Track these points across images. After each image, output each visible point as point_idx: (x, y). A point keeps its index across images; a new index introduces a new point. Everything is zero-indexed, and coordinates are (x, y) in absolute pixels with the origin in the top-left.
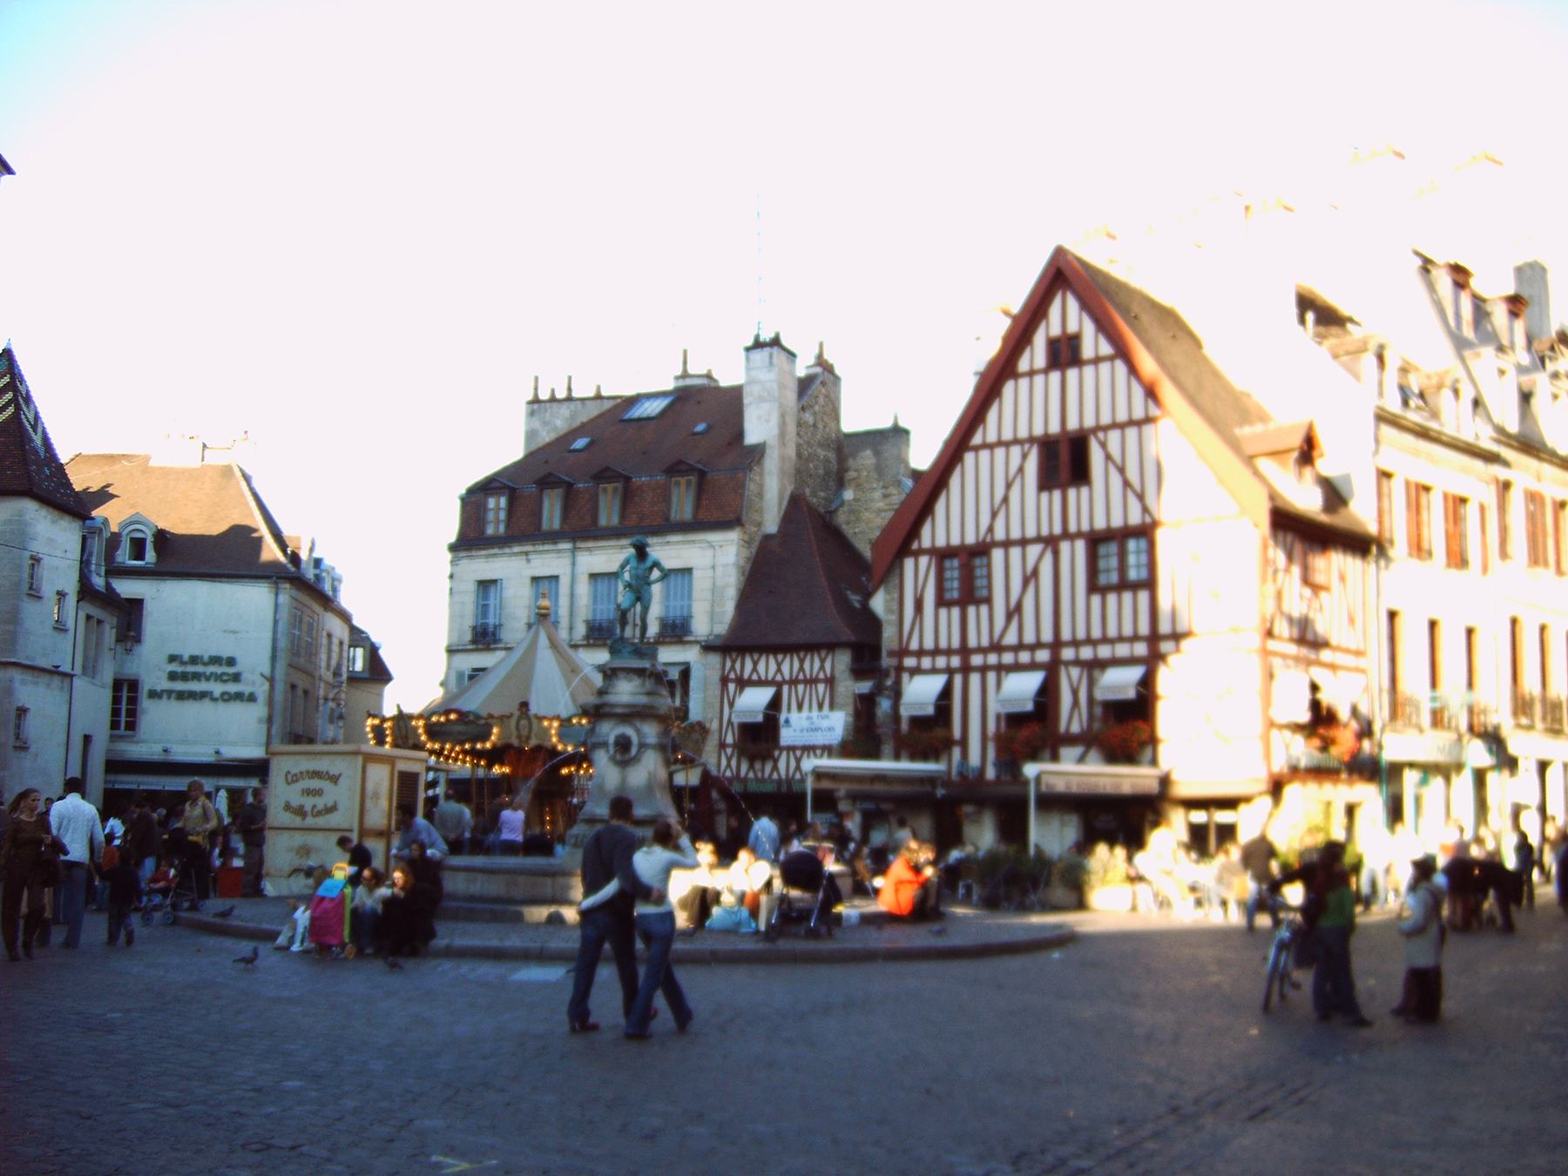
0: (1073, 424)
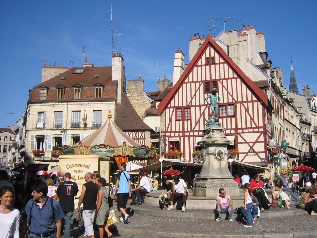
0: (213, 78)
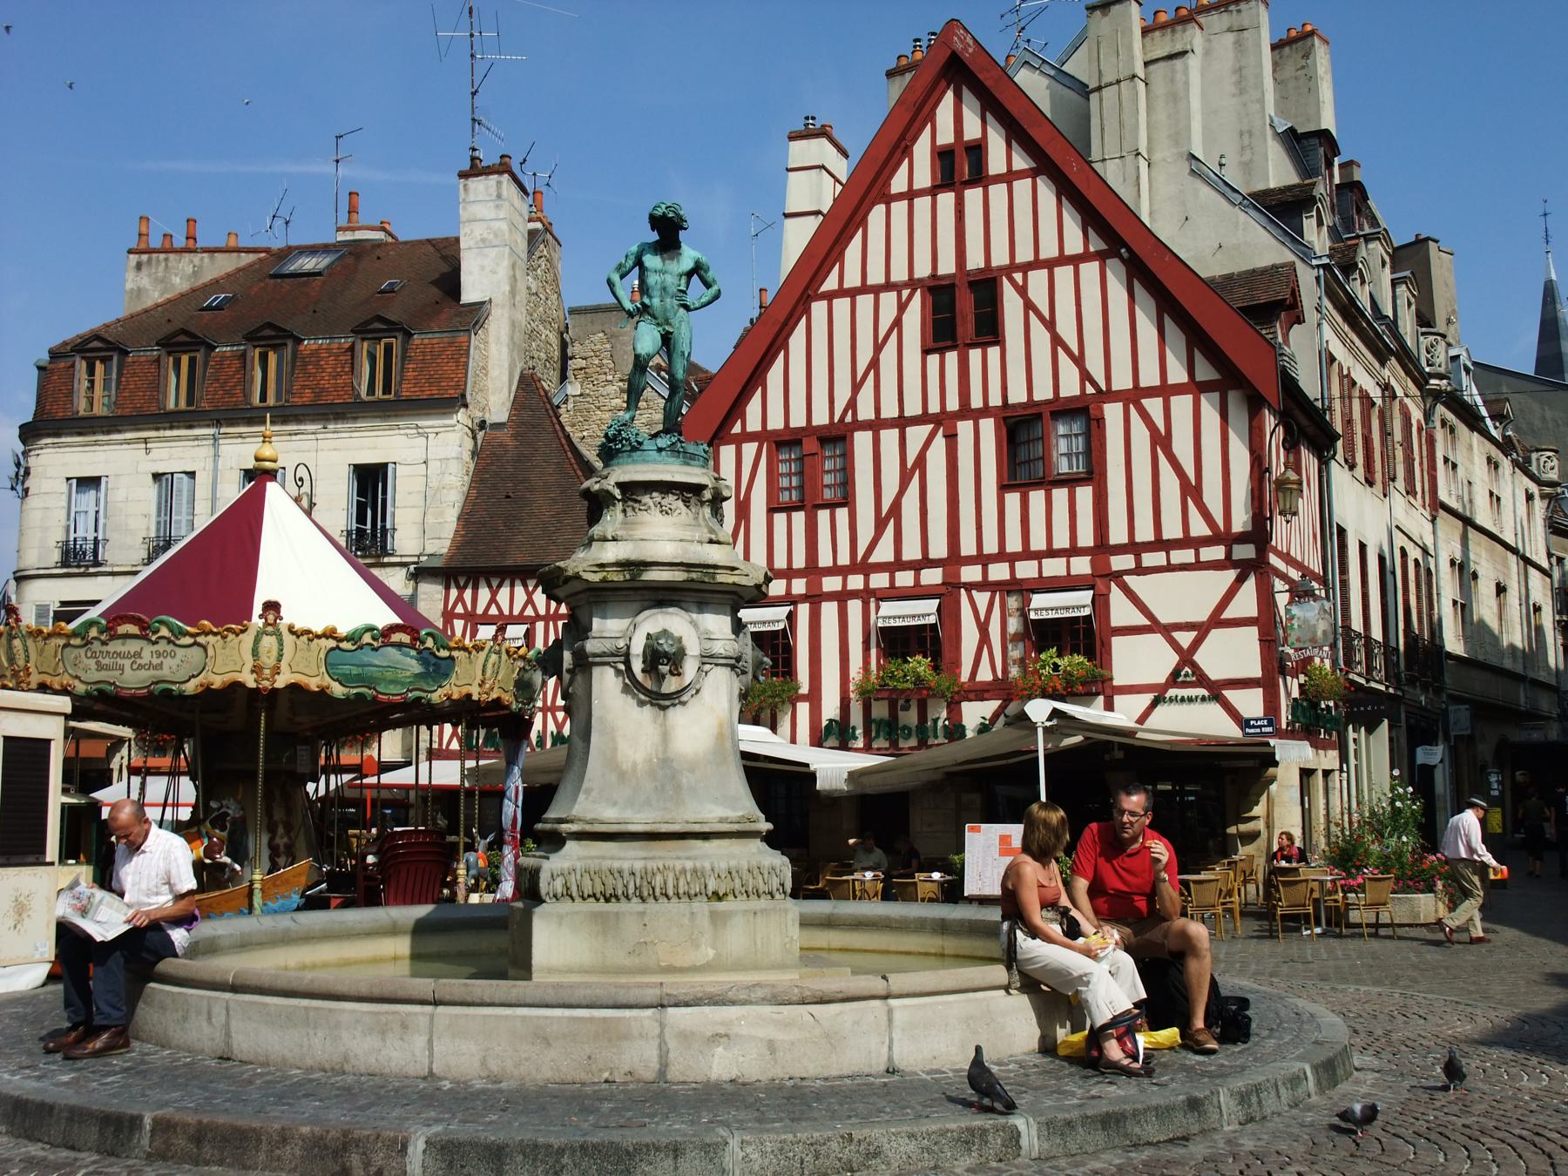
0: (975, 261)
